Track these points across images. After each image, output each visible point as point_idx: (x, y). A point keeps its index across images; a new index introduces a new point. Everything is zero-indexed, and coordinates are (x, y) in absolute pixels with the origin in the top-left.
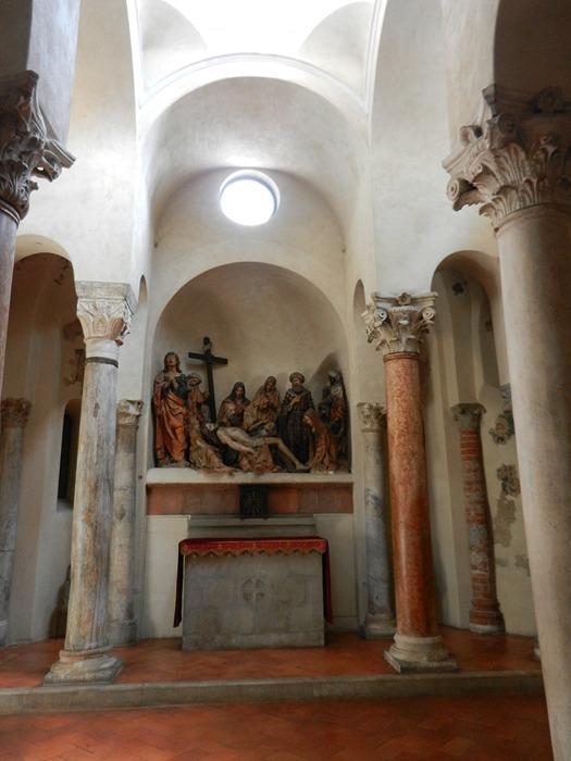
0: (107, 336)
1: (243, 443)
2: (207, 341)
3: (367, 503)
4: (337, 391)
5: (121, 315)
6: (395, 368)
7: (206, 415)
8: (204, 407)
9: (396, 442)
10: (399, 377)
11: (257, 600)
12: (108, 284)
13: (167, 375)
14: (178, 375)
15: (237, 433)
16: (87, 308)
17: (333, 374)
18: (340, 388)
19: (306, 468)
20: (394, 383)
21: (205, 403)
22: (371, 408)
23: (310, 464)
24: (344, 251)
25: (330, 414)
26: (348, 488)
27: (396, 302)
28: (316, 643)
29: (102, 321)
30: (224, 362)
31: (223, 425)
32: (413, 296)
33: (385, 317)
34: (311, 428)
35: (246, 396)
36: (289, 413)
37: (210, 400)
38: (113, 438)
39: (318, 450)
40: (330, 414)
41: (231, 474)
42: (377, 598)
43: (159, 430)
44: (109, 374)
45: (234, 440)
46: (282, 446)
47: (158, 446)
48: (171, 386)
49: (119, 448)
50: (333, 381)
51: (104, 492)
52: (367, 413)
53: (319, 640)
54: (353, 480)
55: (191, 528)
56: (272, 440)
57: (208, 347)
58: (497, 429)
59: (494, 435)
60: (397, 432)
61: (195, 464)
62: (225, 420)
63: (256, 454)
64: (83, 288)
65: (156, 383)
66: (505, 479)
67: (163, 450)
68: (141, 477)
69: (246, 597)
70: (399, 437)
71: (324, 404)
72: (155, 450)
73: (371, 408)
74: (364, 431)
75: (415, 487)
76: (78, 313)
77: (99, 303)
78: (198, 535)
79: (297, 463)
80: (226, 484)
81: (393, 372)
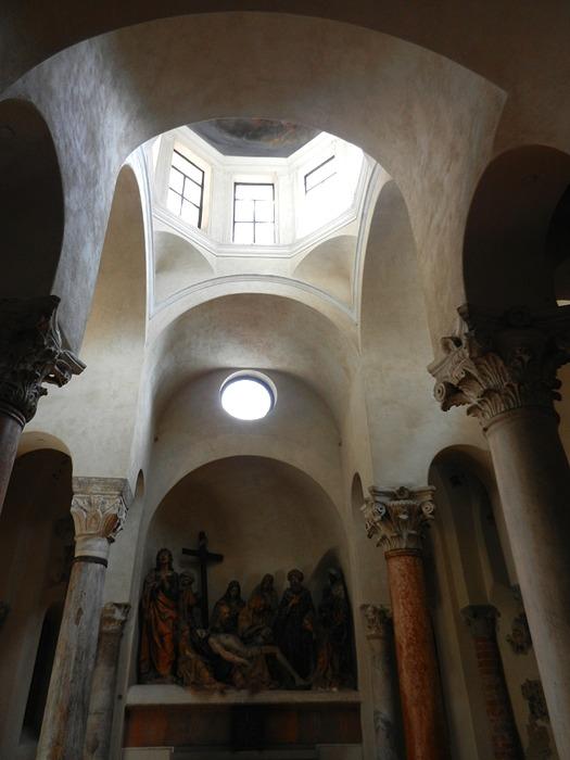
0: (97, 534)
1: (236, 652)
2: (202, 536)
3: (377, 730)
4: (338, 591)
5: (116, 512)
6: (397, 565)
9: (405, 654)
10: (404, 576)
15: (230, 640)
16: (81, 503)
17: (333, 572)
18: (341, 587)
20: (398, 583)
22: (375, 610)
24: (340, 444)
26: (354, 709)
27: (393, 496)
29: (95, 517)
31: (216, 631)
32: (411, 489)
33: (384, 511)
35: (242, 595)
37: (202, 601)
38: (93, 650)
39: (321, 660)
41: (222, 692)
44: (97, 575)
45: (228, 648)
46: (280, 656)
47: (142, 657)
48: (162, 587)
49: (100, 659)
51: (77, 718)
52: (371, 616)
56: (268, 649)
60: (405, 640)
62: (218, 625)
64: (80, 484)
65: (145, 583)
68: (120, 697)
70: (408, 646)
73: (375, 610)
74: (369, 638)
76: (72, 509)
77: (95, 499)
79: (297, 677)
80: (215, 705)
81: (396, 571)
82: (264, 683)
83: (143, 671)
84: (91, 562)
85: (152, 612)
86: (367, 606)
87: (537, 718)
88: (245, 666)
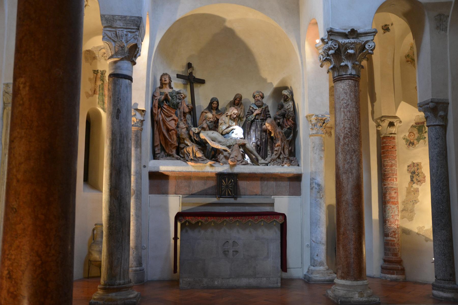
1: (219, 142)
2: (189, 65)
3: (312, 189)
7: (190, 122)
8: (188, 116)
10: (346, 93)
11: (233, 255)
12: (125, 17)
13: (162, 91)
14: (170, 90)
15: (215, 134)
16: (110, 36)
18: (291, 103)
19: (267, 162)
20: (342, 98)
21: (190, 113)
23: (269, 159)
25: (283, 122)
26: (297, 178)
27: (345, 35)
28: (275, 285)
30: (202, 82)
31: (204, 129)
33: (337, 46)
34: (270, 133)
35: (220, 108)
36: (253, 121)
37: (192, 111)
40: (283, 122)
41: (211, 166)
42: (317, 255)
43: (157, 133)
45: (213, 140)
47: (156, 144)
48: (166, 99)
50: (286, 99)
53: (277, 283)
54: (303, 172)
55: (183, 204)
57: (190, 71)
58: (409, 136)
59: (407, 141)
60: (343, 135)
61: (184, 157)
62: (205, 126)
63: (229, 151)
65: (154, 96)
66: (414, 173)
67: (159, 147)
69: (225, 253)
71: (279, 115)
72: (154, 147)
75: (355, 175)
77: (119, 32)
78: (186, 208)
79: (260, 158)
81: (341, 90)
82: (238, 161)
83: (156, 152)
84: (122, 78)
85: (160, 116)
86: (311, 116)
87: (414, 183)
88: (225, 151)
